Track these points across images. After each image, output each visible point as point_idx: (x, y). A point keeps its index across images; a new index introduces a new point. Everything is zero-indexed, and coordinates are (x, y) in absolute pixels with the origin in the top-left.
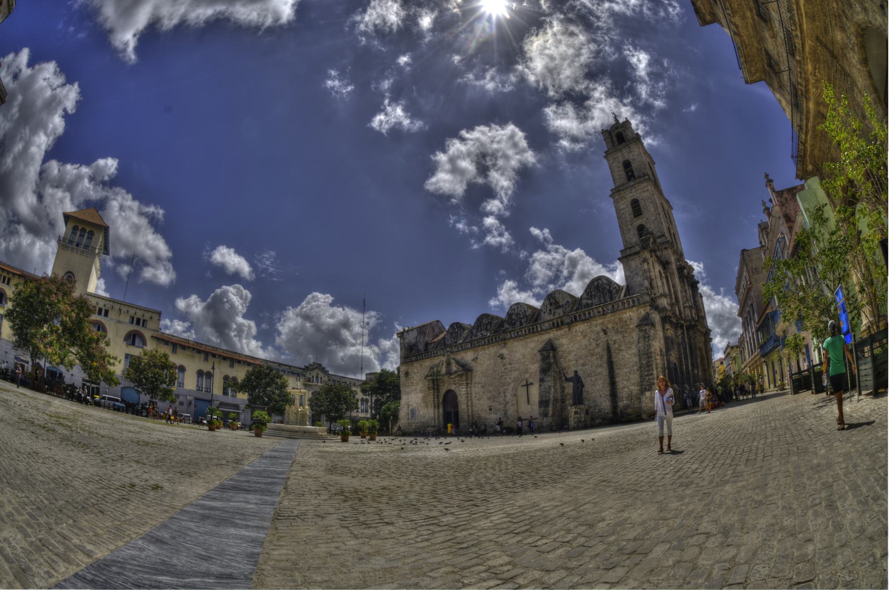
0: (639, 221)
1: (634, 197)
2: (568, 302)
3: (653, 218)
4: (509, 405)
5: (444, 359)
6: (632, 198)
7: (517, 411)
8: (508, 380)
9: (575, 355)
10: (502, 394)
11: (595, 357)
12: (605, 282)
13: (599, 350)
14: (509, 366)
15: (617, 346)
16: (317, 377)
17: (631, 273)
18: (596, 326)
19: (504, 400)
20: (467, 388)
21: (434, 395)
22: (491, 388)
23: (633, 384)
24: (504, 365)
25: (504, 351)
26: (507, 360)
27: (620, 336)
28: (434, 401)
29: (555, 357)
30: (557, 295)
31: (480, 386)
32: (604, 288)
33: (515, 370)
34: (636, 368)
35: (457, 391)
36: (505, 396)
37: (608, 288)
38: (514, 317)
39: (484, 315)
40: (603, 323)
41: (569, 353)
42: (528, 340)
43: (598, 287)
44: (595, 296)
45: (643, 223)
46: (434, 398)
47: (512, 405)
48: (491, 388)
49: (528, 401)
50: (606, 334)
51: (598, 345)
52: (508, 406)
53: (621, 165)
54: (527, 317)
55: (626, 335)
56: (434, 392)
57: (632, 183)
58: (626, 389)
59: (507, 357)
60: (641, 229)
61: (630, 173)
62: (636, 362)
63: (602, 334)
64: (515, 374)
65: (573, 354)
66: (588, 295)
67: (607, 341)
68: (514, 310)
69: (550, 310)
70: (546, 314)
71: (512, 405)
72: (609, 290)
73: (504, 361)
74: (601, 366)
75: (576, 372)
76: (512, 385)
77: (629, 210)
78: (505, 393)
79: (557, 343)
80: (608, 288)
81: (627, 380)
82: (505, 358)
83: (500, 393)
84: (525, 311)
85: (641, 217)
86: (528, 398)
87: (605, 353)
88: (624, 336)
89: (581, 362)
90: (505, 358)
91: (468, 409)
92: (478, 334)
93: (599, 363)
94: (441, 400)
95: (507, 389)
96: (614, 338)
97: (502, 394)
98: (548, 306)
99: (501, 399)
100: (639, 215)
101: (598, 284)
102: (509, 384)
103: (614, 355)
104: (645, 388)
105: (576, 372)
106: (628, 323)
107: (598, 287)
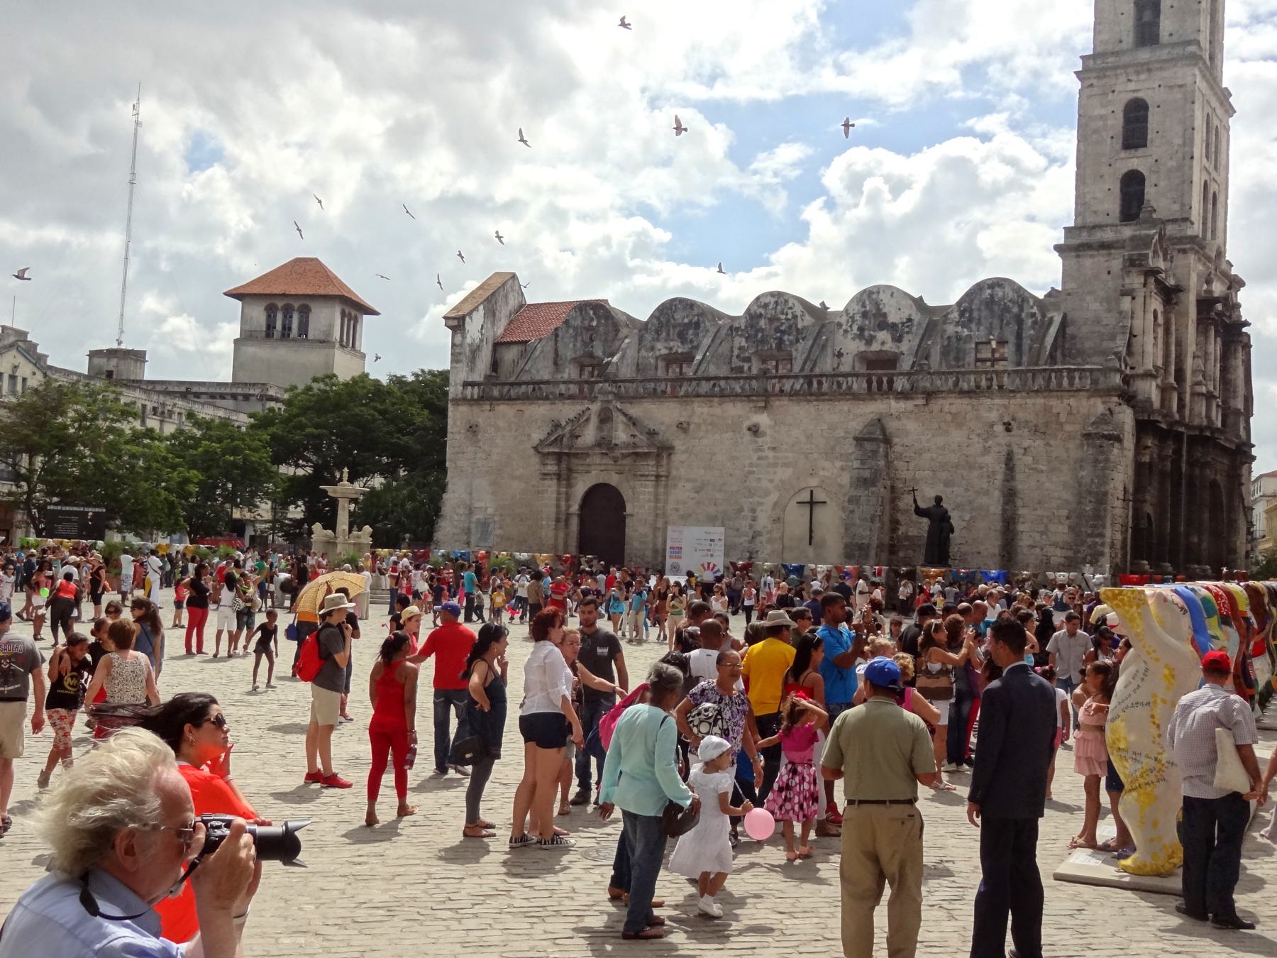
0: (1135, 161)
1: (1140, 95)
2: (909, 320)
3: (1172, 163)
4: (763, 539)
5: (595, 407)
6: (1132, 96)
8: (765, 484)
9: (932, 459)
10: (746, 513)
11: (976, 473)
13: (988, 459)
14: (771, 454)
15: (1029, 459)
16: (13, 378)
18: (990, 410)
19: (751, 527)
20: (657, 486)
21: (559, 493)
22: (719, 496)
23: (1056, 545)
24: (759, 449)
25: (763, 419)
26: (768, 439)
27: (1040, 443)
28: (558, 506)
29: (886, 456)
30: (884, 297)
31: (689, 486)
32: (1006, 309)
33: (785, 465)
34: (1065, 512)
35: (626, 493)
36: (754, 519)
37: (1015, 310)
38: (762, 323)
39: (681, 300)
40: (1006, 407)
41: (919, 453)
43: (990, 302)
44: (979, 323)
46: (558, 500)
47: (770, 541)
48: (719, 496)
49: (811, 537)
50: (1008, 430)
51: (986, 451)
52: (759, 539)
55: (1052, 442)
56: (559, 486)
57: (1144, 55)
58: (1037, 550)
59: (768, 431)
61: (1147, 16)
62: (1067, 501)
63: (999, 428)
64: (784, 474)
65: (927, 456)
66: (962, 314)
67: (1009, 445)
68: (766, 306)
69: (861, 329)
70: (850, 336)
71: (770, 541)
73: (760, 440)
74: (987, 493)
75: (939, 500)
76: (774, 497)
77: (1116, 123)
78: (753, 511)
79: (892, 426)
80: (1015, 310)
81: (1042, 533)
82: (764, 434)
83: (741, 510)
84: (795, 317)
85: (1141, 151)
86: (811, 531)
87: (1000, 469)
88: (1048, 444)
89: (944, 475)
90: (764, 434)
91: (655, 537)
92: (659, 345)
93: (985, 486)
94: (575, 508)
95: (761, 504)
96: (1026, 444)
97: (746, 513)
98: (857, 317)
99: (744, 524)
100: (1136, 147)
101: (992, 296)
102: (767, 493)
103: (1020, 476)
104: (1085, 558)
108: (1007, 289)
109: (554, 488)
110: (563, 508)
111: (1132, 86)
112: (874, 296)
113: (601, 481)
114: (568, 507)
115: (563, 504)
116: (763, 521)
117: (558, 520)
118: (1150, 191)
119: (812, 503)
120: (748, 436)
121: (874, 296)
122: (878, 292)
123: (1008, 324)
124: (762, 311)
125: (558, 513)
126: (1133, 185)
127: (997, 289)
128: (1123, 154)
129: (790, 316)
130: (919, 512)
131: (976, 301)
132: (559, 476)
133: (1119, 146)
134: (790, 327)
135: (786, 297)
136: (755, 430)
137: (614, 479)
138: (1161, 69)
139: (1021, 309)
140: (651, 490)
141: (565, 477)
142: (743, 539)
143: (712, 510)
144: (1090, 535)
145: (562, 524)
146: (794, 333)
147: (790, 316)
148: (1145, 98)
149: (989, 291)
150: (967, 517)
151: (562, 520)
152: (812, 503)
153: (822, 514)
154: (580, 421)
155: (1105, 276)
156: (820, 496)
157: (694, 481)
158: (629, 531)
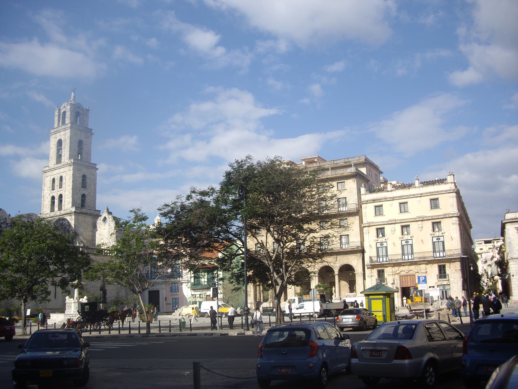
1: (85, 174)
6: (84, 174)
12: (67, 224)
17: (78, 224)
32: (66, 227)
53: (77, 142)
54: (7, 224)
58: (110, 298)
72: (68, 230)
84: (6, 219)
86: (55, 294)
107: (62, 224)
108: (66, 222)
111: (84, 171)
112: (31, 216)
121: (31, 216)
122: (32, 215)
123: (66, 232)
127: (63, 221)
128: (82, 189)
129: (4, 218)
131: (58, 224)
133: (81, 186)
134: (4, 222)
135: (3, 211)
138: (90, 169)
139: (69, 229)
144: (130, 294)
146: (6, 224)
147: (4, 218)
148: (87, 175)
149: (61, 221)
150: (95, 290)
155: (83, 222)
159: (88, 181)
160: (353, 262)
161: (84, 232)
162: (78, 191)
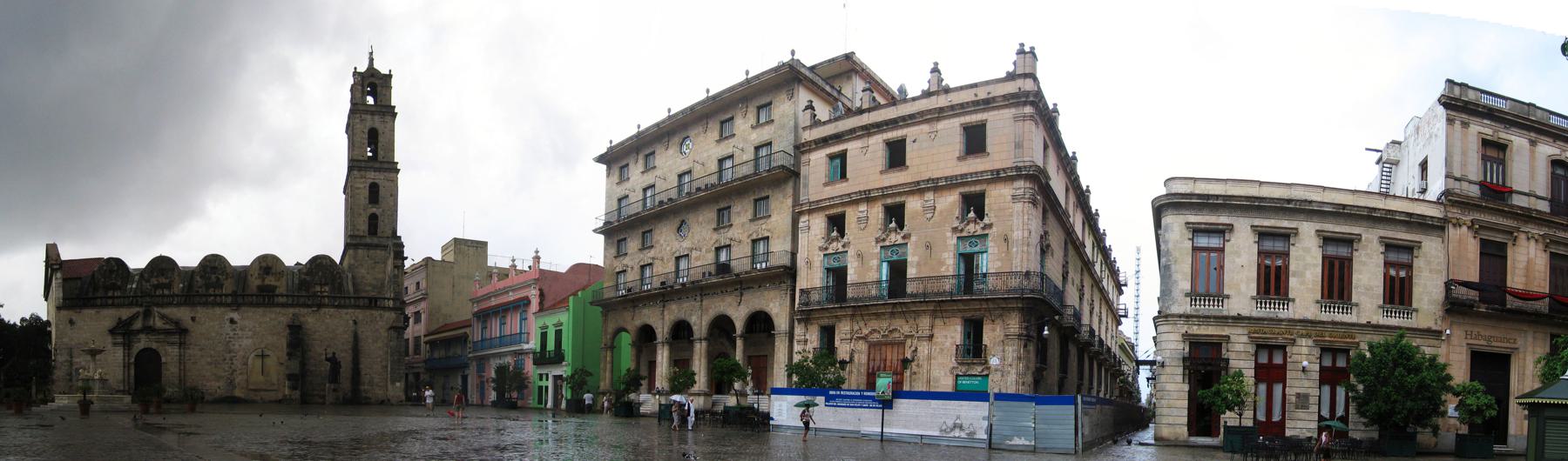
1: (376, 181)
7: (247, 381)
8: (237, 347)
14: (240, 332)
20: (180, 349)
25: (235, 316)
28: (124, 360)
33: (247, 338)
42: (268, 309)
45: (377, 213)
46: (124, 356)
47: (241, 374)
53: (366, 131)
56: (124, 349)
60: (373, 219)
73: (234, 326)
75: (334, 354)
77: (366, 193)
78: (232, 360)
83: (225, 359)
94: (133, 360)
105: (334, 354)
106: (378, 319)
109: (122, 350)
110: (126, 361)
113: (146, 346)
114: (129, 360)
115: (127, 358)
116: (237, 363)
117: (124, 367)
118: (380, 224)
119: (263, 356)
120: (228, 323)
124: (208, 263)
125: (124, 363)
126: (373, 219)
130: (327, 359)
132: (124, 345)
136: (232, 321)
137: (154, 346)
140: (178, 350)
141: (127, 346)
142: (227, 373)
143: (209, 360)
145: (126, 369)
151: (126, 366)
152: (263, 356)
153: (268, 361)
154: (133, 318)
155: (367, 258)
156: (267, 352)
157: (199, 345)
158: (164, 372)
159: (382, 192)
160: (771, 305)
161: (368, 273)
162: (362, 212)
